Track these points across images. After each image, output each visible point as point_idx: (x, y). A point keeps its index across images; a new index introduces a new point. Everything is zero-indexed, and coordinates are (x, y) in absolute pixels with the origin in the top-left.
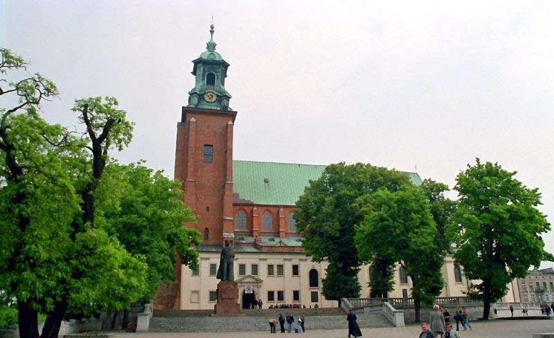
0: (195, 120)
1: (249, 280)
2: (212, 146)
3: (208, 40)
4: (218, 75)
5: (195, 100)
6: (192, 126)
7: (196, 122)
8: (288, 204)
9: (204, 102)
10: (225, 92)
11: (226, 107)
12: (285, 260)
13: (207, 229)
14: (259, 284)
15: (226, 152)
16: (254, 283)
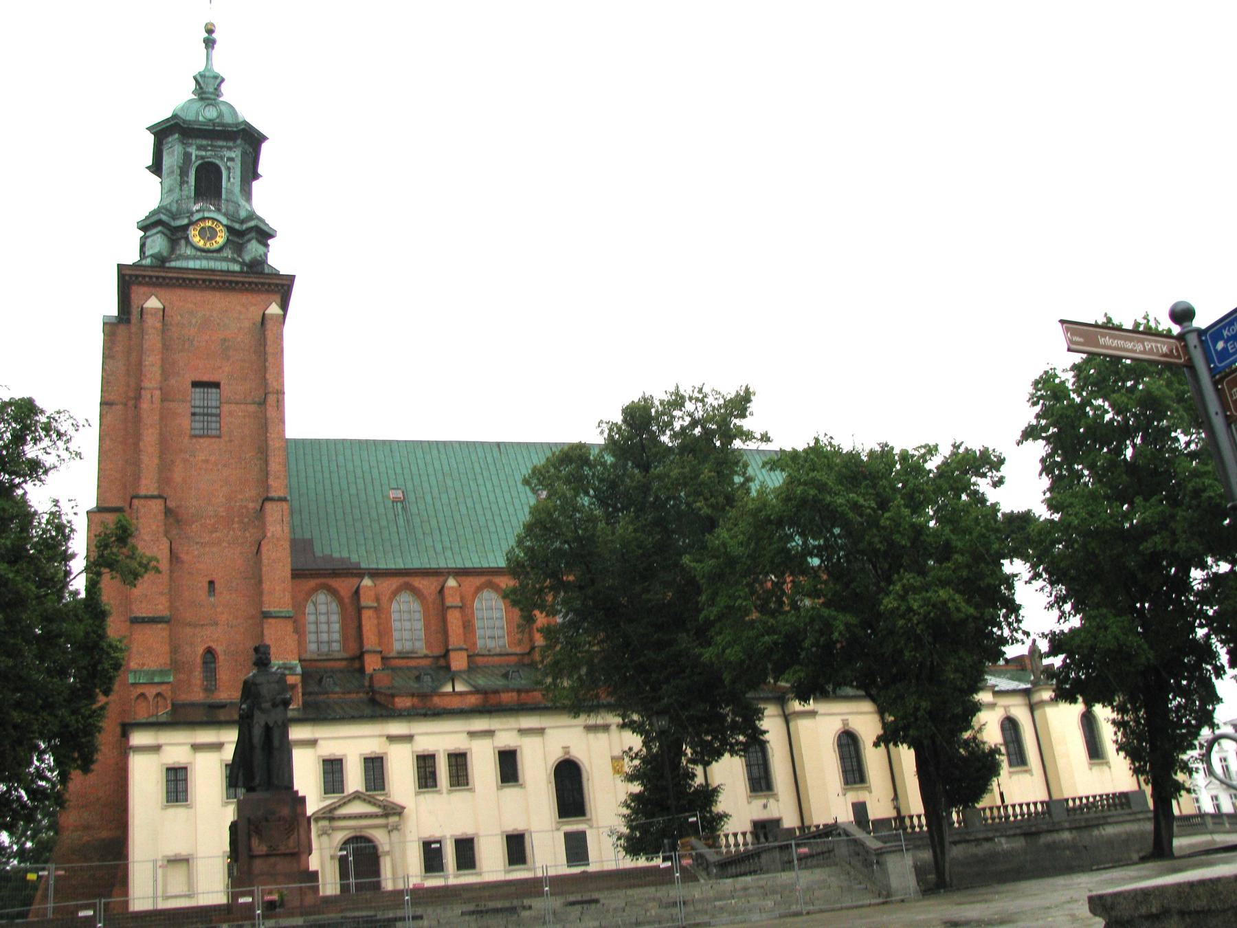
0: (159, 305)
1: (358, 808)
2: (216, 385)
3: (201, 67)
4: (230, 160)
5: (158, 244)
6: (152, 323)
8: (468, 565)
9: (189, 252)
10: (252, 216)
11: (258, 266)
12: (472, 734)
13: (210, 652)
14: (393, 820)
15: (263, 403)
16: (375, 816)
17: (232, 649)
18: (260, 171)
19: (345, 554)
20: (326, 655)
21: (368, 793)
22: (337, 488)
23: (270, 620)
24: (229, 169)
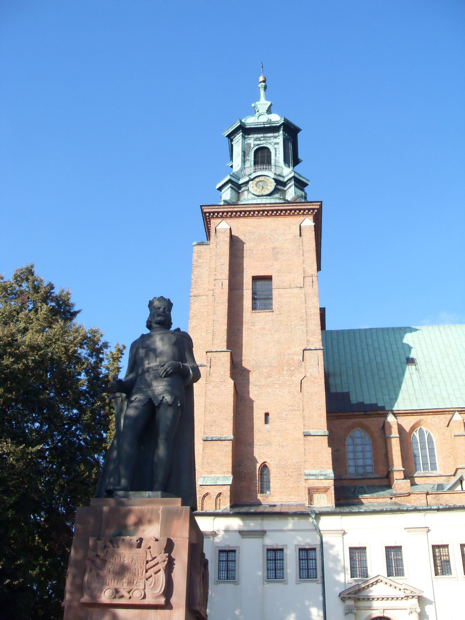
7: (230, 229)
17: (283, 463)
18: (300, 156)
19: (374, 401)
20: (362, 475)
21: (390, 578)
22: (367, 358)
23: (309, 438)
24: (276, 149)
